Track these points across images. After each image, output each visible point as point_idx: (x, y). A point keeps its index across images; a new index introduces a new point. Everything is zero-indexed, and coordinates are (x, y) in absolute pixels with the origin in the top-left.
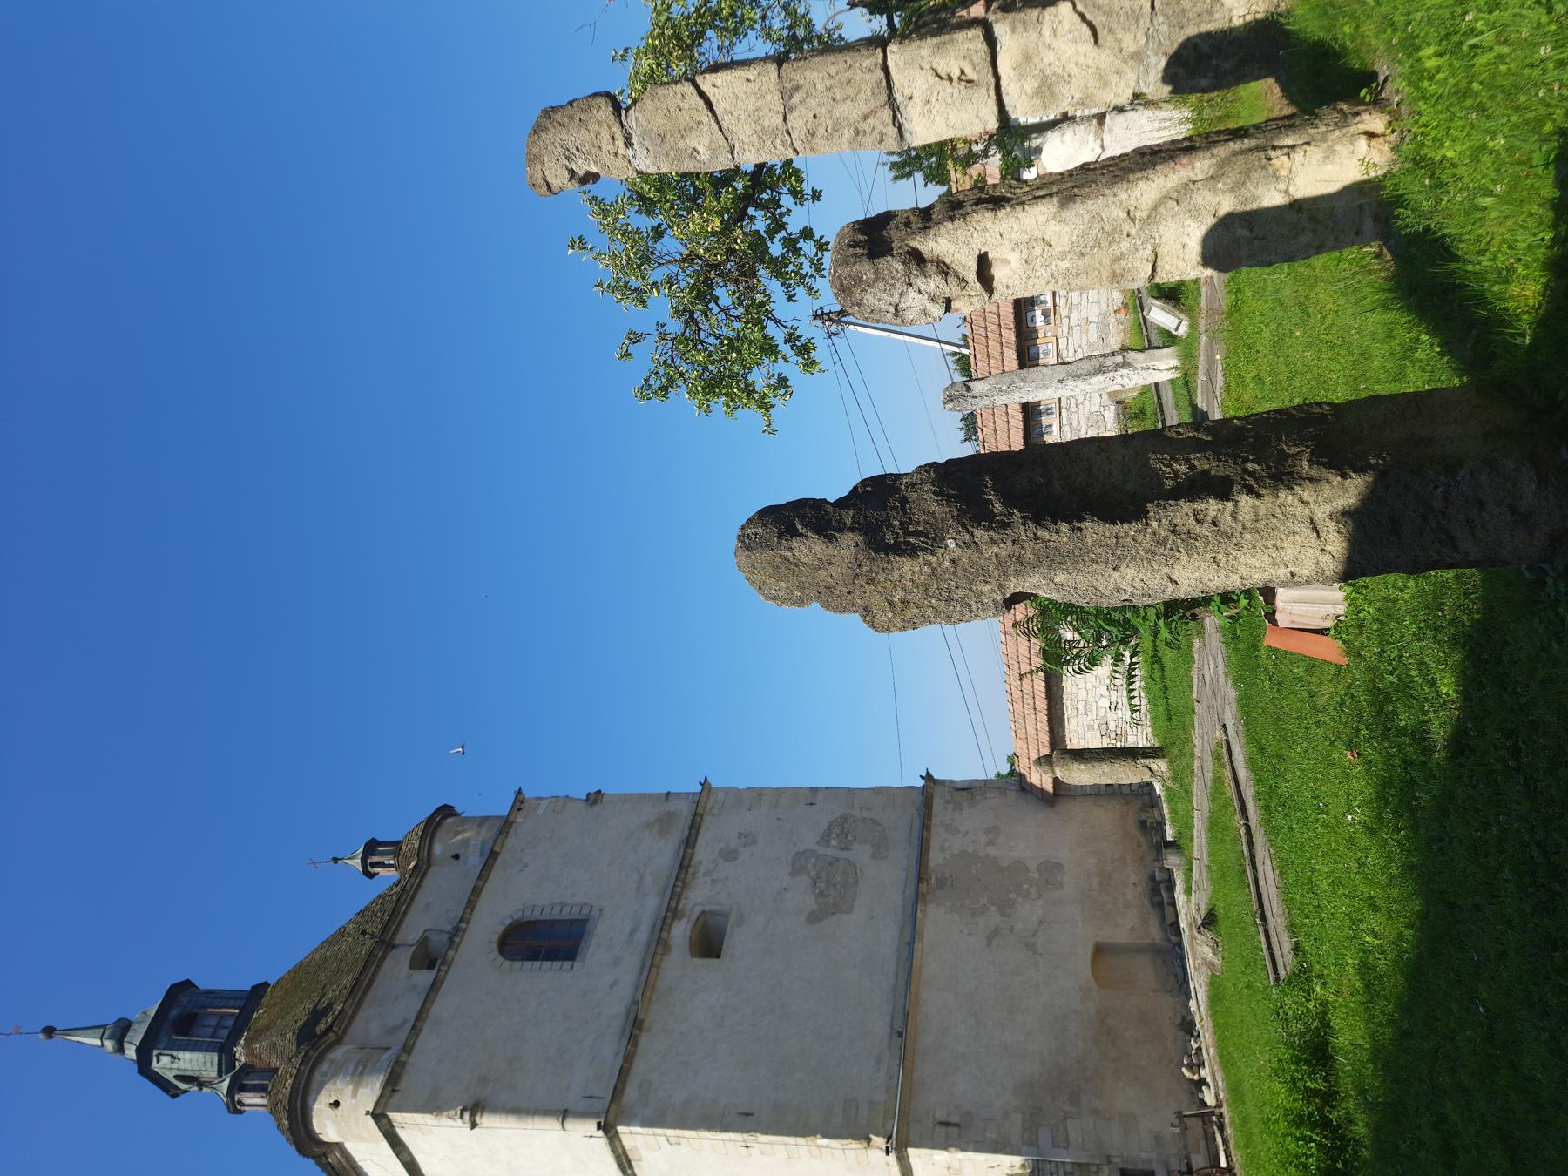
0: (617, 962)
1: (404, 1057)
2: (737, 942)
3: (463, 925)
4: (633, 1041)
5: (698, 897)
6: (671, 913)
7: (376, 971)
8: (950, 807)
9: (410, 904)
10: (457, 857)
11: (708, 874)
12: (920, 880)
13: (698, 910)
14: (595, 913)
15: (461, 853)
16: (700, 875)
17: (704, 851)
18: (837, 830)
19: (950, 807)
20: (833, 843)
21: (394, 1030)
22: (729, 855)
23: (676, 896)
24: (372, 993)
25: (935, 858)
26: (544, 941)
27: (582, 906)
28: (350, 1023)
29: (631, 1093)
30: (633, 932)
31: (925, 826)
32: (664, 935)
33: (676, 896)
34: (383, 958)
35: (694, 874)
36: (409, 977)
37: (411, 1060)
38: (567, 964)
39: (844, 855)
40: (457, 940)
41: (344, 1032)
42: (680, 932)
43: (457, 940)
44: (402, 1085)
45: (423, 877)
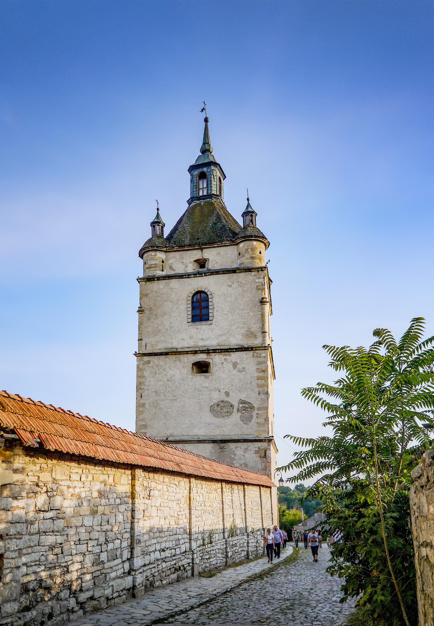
0: (191, 338)
1: (156, 279)
2: (200, 378)
3: (204, 275)
4: (161, 354)
5: (215, 360)
6: (208, 352)
7: (191, 249)
8: (257, 449)
9: (219, 246)
10: (240, 254)
11: (226, 360)
12: (221, 441)
13: (210, 361)
14: (209, 322)
15: (241, 256)
16: (225, 357)
17: (235, 356)
18: (247, 406)
19: (257, 449)
20: (241, 405)
21: (171, 268)
22: (235, 365)
23: (215, 351)
24: (184, 252)
25: (232, 446)
26: (200, 308)
27: (213, 316)
28: (172, 251)
29: (146, 358)
30: (202, 339)
31: (245, 441)
32: (199, 352)
33: (215, 351)
34: (197, 249)
35: (225, 355)
36: (190, 263)
37: (156, 282)
38: (190, 320)
39: (235, 410)
40: (198, 275)
41: (169, 252)
42: (202, 357)
43: (198, 275)
44: (148, 283)
45: (231, 245)
